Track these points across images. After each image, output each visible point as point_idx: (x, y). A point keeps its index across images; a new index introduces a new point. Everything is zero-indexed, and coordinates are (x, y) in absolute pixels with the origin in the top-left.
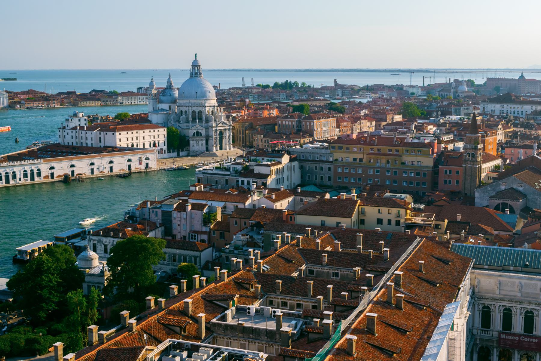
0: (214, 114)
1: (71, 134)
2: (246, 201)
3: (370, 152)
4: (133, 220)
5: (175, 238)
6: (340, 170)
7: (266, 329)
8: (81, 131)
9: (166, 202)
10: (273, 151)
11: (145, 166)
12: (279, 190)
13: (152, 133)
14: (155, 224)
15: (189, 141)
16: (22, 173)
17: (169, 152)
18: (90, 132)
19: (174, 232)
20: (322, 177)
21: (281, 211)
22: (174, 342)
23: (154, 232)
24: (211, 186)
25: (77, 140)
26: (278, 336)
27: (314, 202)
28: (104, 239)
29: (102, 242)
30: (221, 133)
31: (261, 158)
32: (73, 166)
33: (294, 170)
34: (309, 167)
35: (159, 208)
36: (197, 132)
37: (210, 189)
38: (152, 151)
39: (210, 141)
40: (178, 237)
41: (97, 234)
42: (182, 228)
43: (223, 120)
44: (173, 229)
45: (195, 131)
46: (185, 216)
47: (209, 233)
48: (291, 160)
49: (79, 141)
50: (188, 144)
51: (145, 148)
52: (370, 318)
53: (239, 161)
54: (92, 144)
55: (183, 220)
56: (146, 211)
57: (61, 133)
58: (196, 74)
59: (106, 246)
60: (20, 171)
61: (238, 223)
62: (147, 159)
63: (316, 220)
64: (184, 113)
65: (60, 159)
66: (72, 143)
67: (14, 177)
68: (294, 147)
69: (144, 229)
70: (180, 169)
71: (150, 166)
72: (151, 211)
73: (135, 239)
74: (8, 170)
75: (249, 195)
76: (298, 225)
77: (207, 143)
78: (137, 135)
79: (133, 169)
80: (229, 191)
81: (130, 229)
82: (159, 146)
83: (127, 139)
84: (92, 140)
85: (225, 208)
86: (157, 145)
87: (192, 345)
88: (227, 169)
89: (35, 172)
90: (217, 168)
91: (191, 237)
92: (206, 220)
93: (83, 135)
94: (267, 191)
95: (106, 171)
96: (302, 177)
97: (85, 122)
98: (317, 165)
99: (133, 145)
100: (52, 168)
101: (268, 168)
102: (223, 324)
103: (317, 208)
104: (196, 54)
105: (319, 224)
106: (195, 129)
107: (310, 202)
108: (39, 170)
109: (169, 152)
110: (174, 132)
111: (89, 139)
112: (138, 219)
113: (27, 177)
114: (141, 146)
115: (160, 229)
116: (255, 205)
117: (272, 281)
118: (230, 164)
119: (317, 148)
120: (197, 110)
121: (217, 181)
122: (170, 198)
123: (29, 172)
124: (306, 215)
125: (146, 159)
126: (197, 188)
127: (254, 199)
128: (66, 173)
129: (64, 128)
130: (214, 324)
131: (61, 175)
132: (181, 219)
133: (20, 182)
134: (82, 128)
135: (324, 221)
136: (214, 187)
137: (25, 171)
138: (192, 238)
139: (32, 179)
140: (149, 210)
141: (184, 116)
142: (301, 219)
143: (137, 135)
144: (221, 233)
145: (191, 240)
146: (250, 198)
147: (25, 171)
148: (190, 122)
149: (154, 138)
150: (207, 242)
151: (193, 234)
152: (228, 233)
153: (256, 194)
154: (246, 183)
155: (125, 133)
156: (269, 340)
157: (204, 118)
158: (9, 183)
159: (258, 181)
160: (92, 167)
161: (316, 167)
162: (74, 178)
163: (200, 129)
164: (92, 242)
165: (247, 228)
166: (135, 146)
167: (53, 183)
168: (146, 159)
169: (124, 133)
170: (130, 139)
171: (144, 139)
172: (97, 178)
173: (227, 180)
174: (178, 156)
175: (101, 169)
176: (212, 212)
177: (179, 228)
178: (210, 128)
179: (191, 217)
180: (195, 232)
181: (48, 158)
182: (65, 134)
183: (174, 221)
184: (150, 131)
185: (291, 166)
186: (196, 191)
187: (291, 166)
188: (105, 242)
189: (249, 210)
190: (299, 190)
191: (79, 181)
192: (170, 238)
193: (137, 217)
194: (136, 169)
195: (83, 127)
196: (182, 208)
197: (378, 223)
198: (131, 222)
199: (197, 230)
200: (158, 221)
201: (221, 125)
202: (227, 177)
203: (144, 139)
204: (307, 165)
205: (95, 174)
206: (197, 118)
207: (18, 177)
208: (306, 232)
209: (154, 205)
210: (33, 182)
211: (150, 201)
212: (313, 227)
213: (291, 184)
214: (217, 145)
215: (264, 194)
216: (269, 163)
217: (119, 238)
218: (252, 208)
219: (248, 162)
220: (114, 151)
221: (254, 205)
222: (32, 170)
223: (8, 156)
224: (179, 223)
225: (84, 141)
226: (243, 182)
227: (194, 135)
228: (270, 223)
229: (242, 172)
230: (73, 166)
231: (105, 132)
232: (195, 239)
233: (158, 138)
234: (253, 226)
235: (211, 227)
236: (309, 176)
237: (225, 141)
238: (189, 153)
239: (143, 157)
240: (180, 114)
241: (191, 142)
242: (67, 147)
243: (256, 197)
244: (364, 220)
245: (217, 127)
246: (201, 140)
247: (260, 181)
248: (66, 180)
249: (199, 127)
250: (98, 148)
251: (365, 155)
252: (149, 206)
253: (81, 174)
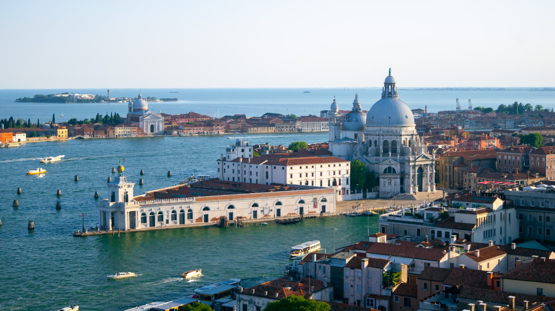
1: (232, 167)
2: (441, 258)
4: (294, 277)
5: (347, 303)
8: (244, 164)
9: (335, 257)
10: (483, 194)
11: (321, 210)
12: (487, 245)
13: (332, 168)
14: (321, 283)
15: (378, 179)
16: (170, 213)
17: (353, 192)
18: (255, 165)
19: (346, 295)
20: (548, 231)
21: (485, 272)
23: (319, 293)
24: (398, 237)
25: (240, 175)
27: (528, 264)
28: (257, 300)
29: (254, 303)
30: (421, 170)
31: (465, 203)
32: (231, 207)
33: (509, 220)
34: (531, 216)
35: (328, 263)
37: (397, 241)
38: (329, 191)
39: (406, 180)
40: (351, 301)
41: (248, 293)
42: (356, 290)
43: (423, 153)
44: (345, 290)
45: (387, 166)
46: (360, 275)
47: (390, 299)
48: (505, 206)
49: (242, 176)
50: (377, 183)
51: (323, 186)
53: (436, 206)
54: (257, 180)
55: (357, 280)
56: (311, 266)
57: (220, 166)
58: (390, 93)
60: (168, 212)
61: (428, 286)
62: (324, 200)
63: (531, 287)
64: (373, 143)
65: (217, 199)
66: (234, 178)
67: (161, 218)
68: (511, 190)
69: (306, 289)
70: (365, 215)
71: (327, 210)
72: (318, 265)
73: (291, 300)
74: (153, 211)
75: (445, 251)
76: (503, 292)
77: (402, 182)
78: (313, 170)
79: (306, 212)
81: (290, 288)
82: (340, 184)
83: (301, 175)
84: (257, 175)
85: (412, 266)
86: (338, 183)
88: (419, 216)
89: (186, 213)
90: (407, 214)
91: (367, 302)
92: (387, 282)
93: (247, 169)
94: (469, 246)
95: (273, 215)
96: (520, 230)
97: (250, 153)
98: (542, 215)
99: (307, 184)
100: (207, 209)
101: (474, 216)
103: (532, 271)
104: (390, 69)
105: (535, 292)
106: (387, 164)
107: (524, 262)
108: (190, 210)
109: (353, 192)
110: (360, 167)
111: (254, 173)
112: (301, 276)
113: (176, 219)
114: (317, 184)
115: (327, 290)
116: (453, 264)
118: (424, 209)
119: (542, 191)
120: (390, 139)
121: (406, 231)
122: (343, 251)
123: (178, 213)
124: (516, 279)
125: (322, 201)
126: (379, 238)
127: (451, 256)
128: (222, 215)
129: (224, 159)
131: (218, 217)
132: (355, 278)
133: (167, 225)
134: (245, 160)
135: (542, 289)
136: (401, 239)
137: (174, 212)
138: (368, 304)
139: (182, 221)
140: (315, 265)
141: (373, 147)
142: (509, 285)
143: (313, 170)
144: (406, 299)
145: (367, 307)
146: (446, 256)
147: (174, 212)
148: (381, 155)
149: (334, 174)
151: (370, 299)
152: (415, 299)
153: (454, 249)
155: (298, 166)
157: (399, 150)
158: (154, 225)
159: (460, 233)
160: (255, 209)
161: (540, 217)
162: (229, 222)
164: (242, 302)
165: (439, 293)
166: (310, 184)
167: (206, 227)
168: (322, 201)
169: (296, 168)
170: (304, 175)
171: (321, 175)
172: (261, 224)
173: (419, 230)
174: (365, 197)
175: (266, 212)
176: (395, 269)
177: (351, 290)
178: (406, 163)
179: (368, 277)
180: (372, 296)
181: (202, 196)
182: (225, 167)
183: (346, 281)
184: (329, 166)
185: (505, 214)
186: (377, 243)
187: (505, 214)
188: (258, 303)
189: (444, 270)
190: (514, 246)
191: (238, 225)
192: (340, 302)
193: (300, 274)
194: (310, 212)
195: (247, 159)
196: (356, 264)
198: (292, 279)
199: (376, 293)
200: (325, 279)
201: (420, 159)
202: (419, 226)
203: (321, 175)
204: (527, 214)
205: (258, 218)
206: (390, 149)
207: (165, 218)
208: (509, 301)
209: (323, 259)
210: (182, 226)
211: (317, 254)
212: (520, 297)
213: (505, 238)
214: (415, 185)
215: (466, 251)
216: (474, 209)
217: (275, 299)
218: (449, 268)
219: (447, 207)
220: (283, 190)
221: (452, 265)
222: (182, 211)
223: (155, 193)
224: (352, 283)
225: (247, 176)
226: (440, 234)
227: (385, 171)
228: (467, 289)
229: (440, 220)
230: (231, 207)
231: (273, 166)
232: (372, 305)
233: (340, 174)
234: (447, 291)
235: (393, 291)
236: (530, 229)
238: (378, 195)
239: (319, 197)
240: (369, 144)
241: (381, 180)
242: (227, 183)
243: (454, 254)
245: (415, 161)
246: (394, 178)
247: (462, 233)
248: (222, 224)
249: (393, 162)
250: (264, 185)
252: (315, 260)
253: (241, 218)
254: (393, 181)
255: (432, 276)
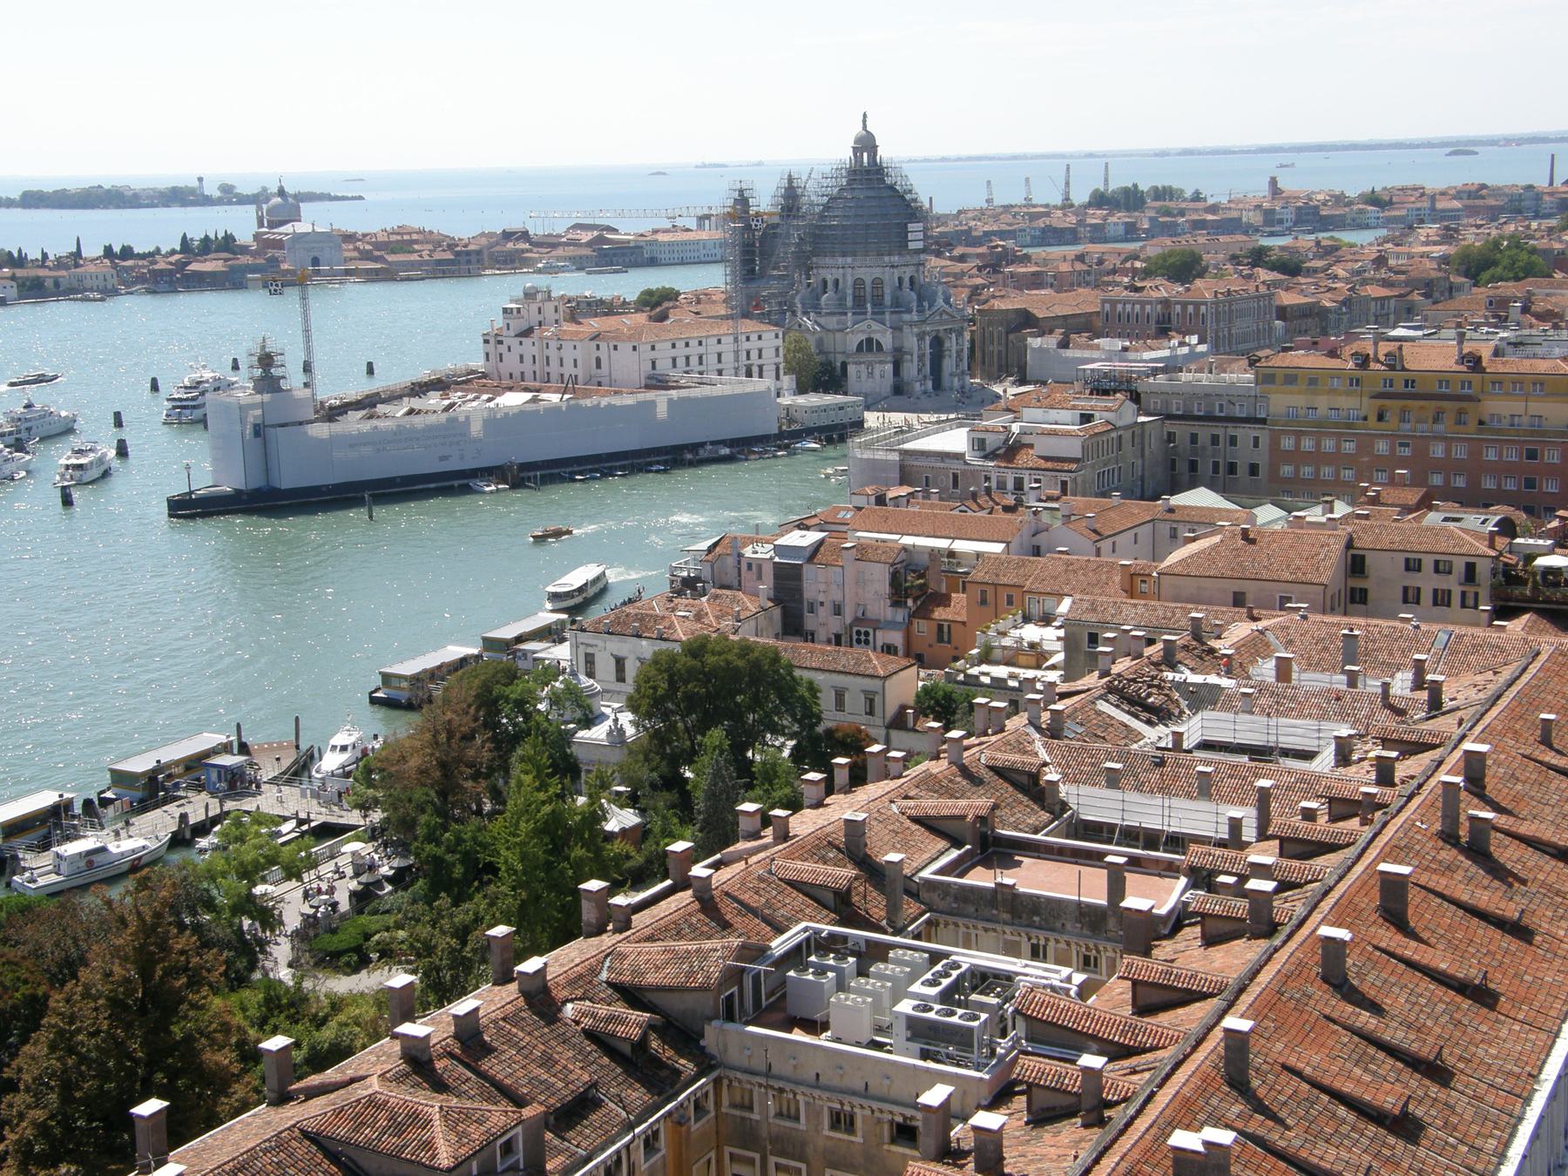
0: (916, 287)
1: (517, 350)
3: (1381, 389)
4: (694, 589)
6: (1287, 443)
7: (1079, 903)
15: (844, 365)
19: (810, 622)
22: (817, 932)
25: (537, 368)
26: (1112, 923)
36: (869, 341)
40: (822, 634)
45: (863, 337)
52: (1390, 878)
59: (620, 663)
64: (830, 285)
66: (522, 373)
78: (701, 350)
80: (963, 508)
83: (674, 360)
87: (868, 941)
91: (855, 637)
98: (1219, 431)
102: (955, 884)
111: (569, 363)
116: (1038, 547)
117: (1093, 764)
130: (927, 882)
138: (859, 641)
140: (739, 562)
149: (748, 358)
150: (900, 653)
154: (1010, 485)
156: (1085, 932)
157: (888, 300)
163: (878, 331)
171: (720, 361)
173: (955, 477)
178: (906, 329)
193: (704, 582)
197: (1405, 601)
203: (719, 361)
224: (821, 598)
226: (1002, 486)
227: (860, 348)
232: (867, 642)
237: (948, 365)
244: (1366, 590)
245: (923, 322)
246: (881, 362)
249: (875, 326)
251: (1365, 400)
254: (878, 369)
255: (997, 575)
